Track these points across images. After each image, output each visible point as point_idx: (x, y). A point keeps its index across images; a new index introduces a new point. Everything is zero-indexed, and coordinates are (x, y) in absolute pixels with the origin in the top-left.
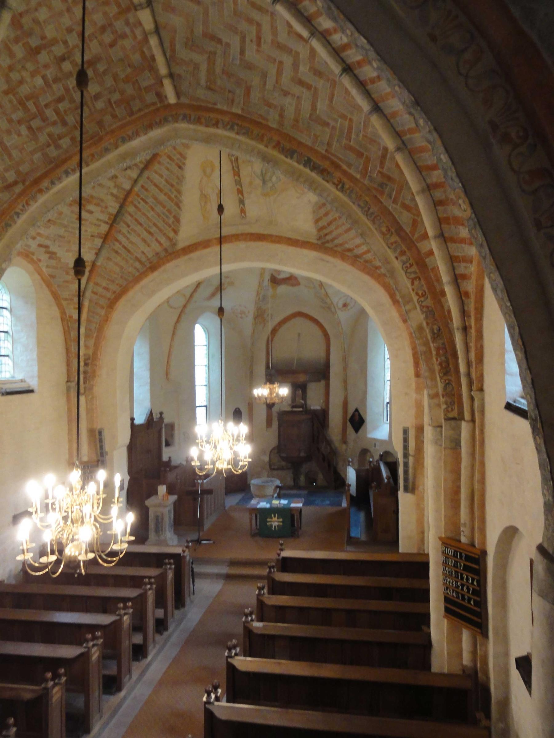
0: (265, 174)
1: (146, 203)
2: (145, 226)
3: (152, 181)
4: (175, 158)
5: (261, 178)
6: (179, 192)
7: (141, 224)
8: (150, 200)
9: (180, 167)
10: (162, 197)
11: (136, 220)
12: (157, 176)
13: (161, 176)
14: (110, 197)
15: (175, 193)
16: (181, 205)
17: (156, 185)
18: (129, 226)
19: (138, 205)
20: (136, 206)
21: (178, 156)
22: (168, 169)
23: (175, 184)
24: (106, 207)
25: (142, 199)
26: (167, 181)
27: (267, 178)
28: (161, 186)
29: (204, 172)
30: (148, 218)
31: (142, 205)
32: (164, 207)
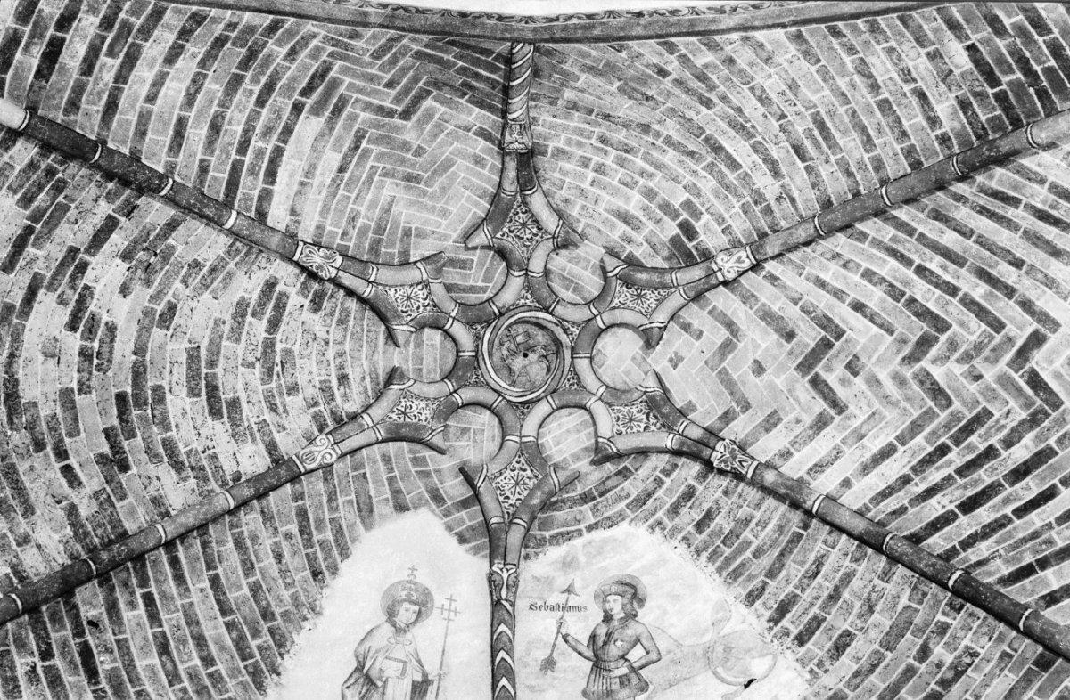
0: (605, 643)
1: (154, 617)
2: (104, 684)
3: (210, 565)
4: (316, 536)
5: (589, 653)
6: (281, 642)
7: (92, 673)
8: (171, 618)
9: (316, 574)
10: (213, 628)
11: (86, 652)
12: (234, 558)
13: (249, 568)
14: (60, 513)
15: (266, 638)
16: (270, 680)
17: (215, 581)
18: (46, 654)
19: (122, 605)
20: (112, 608)
21: (329, 535)
22: (279, 557)
23: (278, 611)
24: (24, 540)
25: (149, 599)
26: (255, 589)
27: (614, 650)
28: (232, 596)
29: (391, 614)
30: (130, 666)
31: (135, 616)
32: (208, 661)
